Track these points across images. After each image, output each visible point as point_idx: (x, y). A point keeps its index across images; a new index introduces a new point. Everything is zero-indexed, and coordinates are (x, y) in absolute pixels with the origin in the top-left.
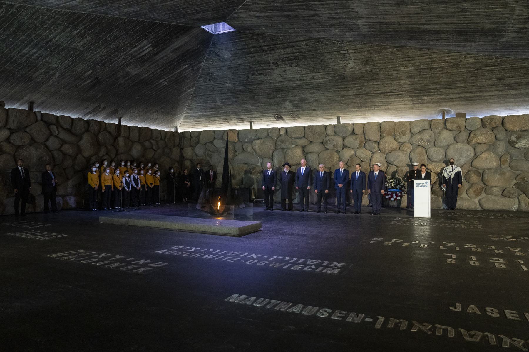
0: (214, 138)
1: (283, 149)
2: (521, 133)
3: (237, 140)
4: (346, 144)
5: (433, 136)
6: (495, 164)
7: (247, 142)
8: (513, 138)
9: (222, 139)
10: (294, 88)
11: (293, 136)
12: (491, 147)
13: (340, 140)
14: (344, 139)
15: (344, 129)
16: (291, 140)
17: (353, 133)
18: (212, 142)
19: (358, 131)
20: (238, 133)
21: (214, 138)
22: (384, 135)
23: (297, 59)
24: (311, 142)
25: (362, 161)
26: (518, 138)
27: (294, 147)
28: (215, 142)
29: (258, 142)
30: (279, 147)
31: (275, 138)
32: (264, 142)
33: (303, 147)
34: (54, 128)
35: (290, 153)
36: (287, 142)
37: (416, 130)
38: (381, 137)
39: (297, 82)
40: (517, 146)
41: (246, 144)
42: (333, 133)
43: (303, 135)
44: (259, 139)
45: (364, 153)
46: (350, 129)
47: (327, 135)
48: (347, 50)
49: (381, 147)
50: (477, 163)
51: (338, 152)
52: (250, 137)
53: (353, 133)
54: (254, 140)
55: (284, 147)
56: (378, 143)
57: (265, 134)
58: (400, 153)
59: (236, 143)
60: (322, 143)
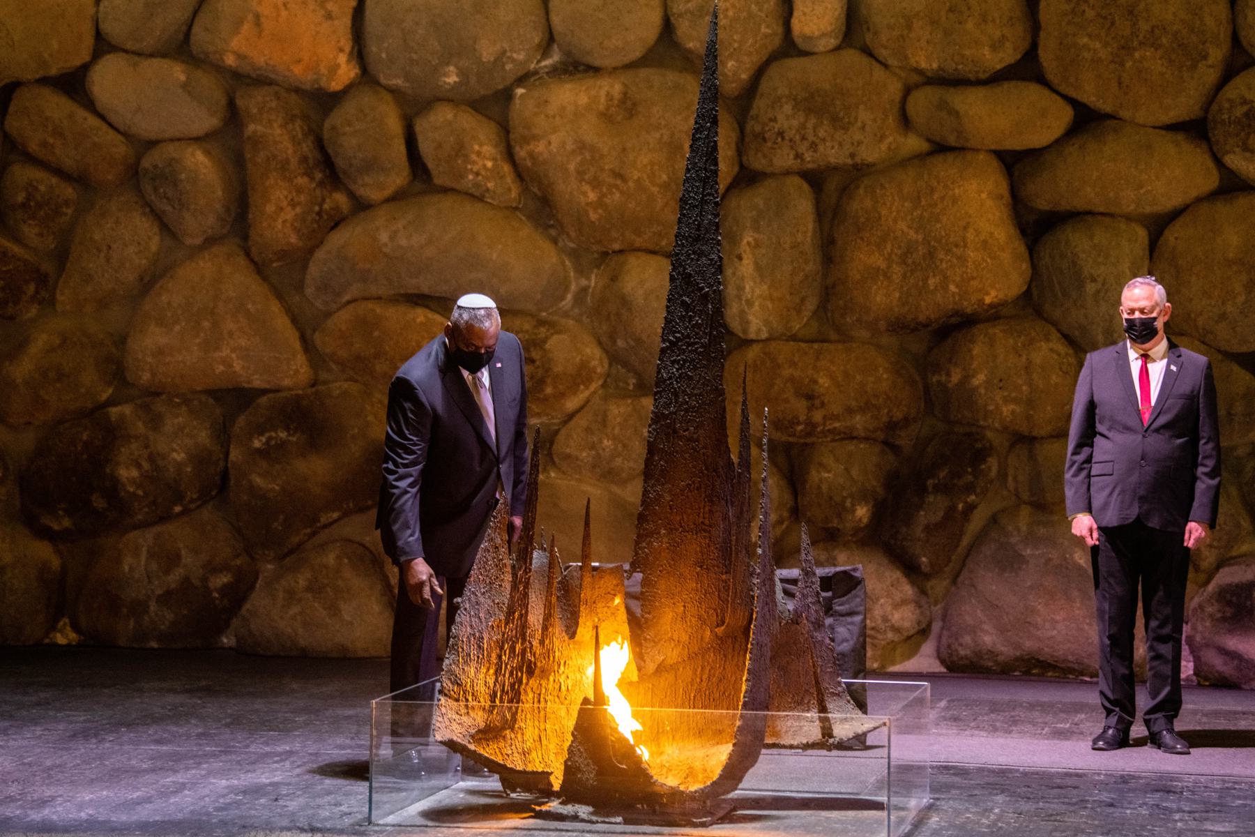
1: (815, 179)
3: (346, 72)
7: (450, 98)
11: (926, 60)
16: (894, 88)
18: (73, 84)
21: (103, 45)
27: (921, 157)
28: (108, 80)
29: (569, 95)
30: (784, 159)
31: (734, 70)
32: (629, 107)
33: (1016, 164)
35: (891, 208)
36: (864, 115)
41: (443, 115)
43: (1008, 56)
44: (577, 67)
52: (487, 52)
54: (521, 80)
55: (833, 153)
59: (324, 101)
60: (1196, 129)
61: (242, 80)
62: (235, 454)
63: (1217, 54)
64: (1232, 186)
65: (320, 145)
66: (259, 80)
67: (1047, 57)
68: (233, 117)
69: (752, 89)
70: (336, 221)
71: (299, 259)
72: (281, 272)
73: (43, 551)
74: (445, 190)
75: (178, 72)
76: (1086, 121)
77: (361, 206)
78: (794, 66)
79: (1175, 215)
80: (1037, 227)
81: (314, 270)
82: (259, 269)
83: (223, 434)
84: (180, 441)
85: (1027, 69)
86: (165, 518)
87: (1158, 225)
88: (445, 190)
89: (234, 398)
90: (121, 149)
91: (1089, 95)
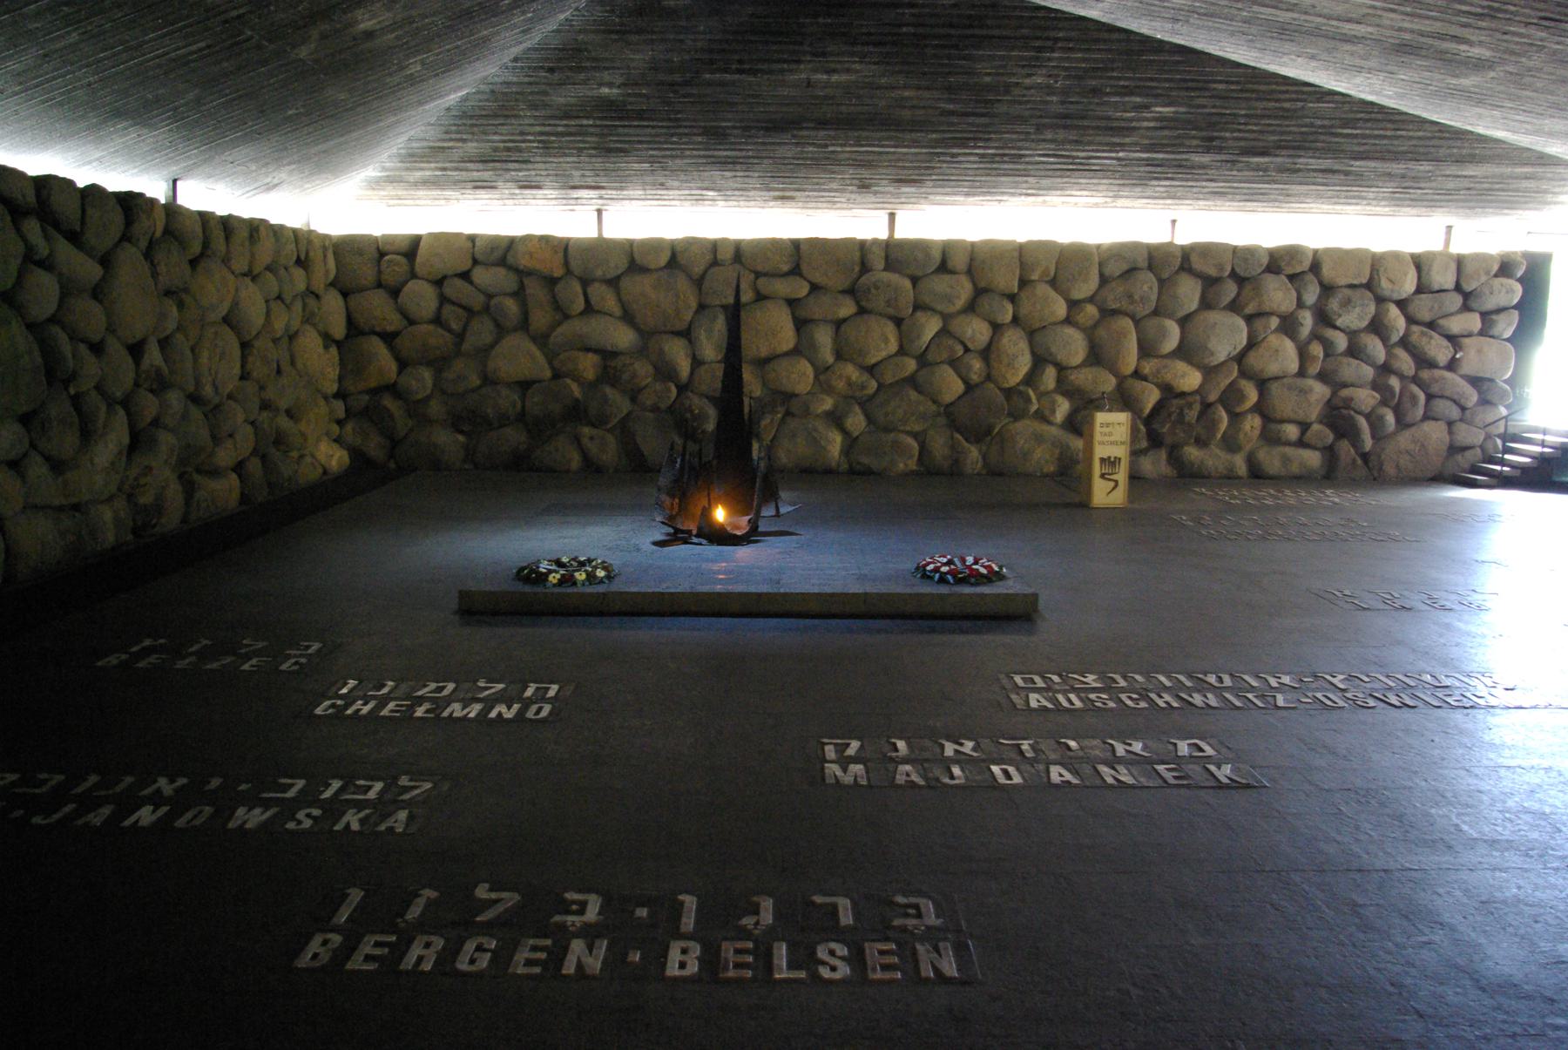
0: (475, 262)
2: (1348, 292)
4: (927, 299)
5: (1156, 290)
6: (1293, 366)
8: (1334, 304)
9: (502, 262)
10: (822, 124)
12: (1288, 326)
13: (907, 284)
14: (915, 280)
15: (920, 256)
17: (944, 267)
19: (959, 262)
20: (564, 248)
22: (1035, 277)
23: (894, 43)
24: (815, 288)
25: (967, 350)
26: (1347, 303)
31: (698, 270)
33: (792, 303)
34: (32, 227)
37: (1114, 269)
38: (1024, 283)
39: (843, 109)
40: (1339, 323)
41: (597, 285)
42: (882, 266)
45: (976, 331)
46: (937, 256)
47: (865, 268)
48: (1056, 40)
49: (1024, 310)
50: (1253, 360)
51: (898, 322)
53: (944, 267)
56: (1012, 298)
57: (664, 259)
58: (1069, 331)
60: (851, 291)
61: (521, 273)
62: (527, 403)
63: (857, 269)
64: (862, 311)
65: (554, 297)
66: (529, 273)
67: (804, 268)
68: (522, 287)
69: (703, 276)
70: (559, 324)
71: (546, 336)
72: (541, 340)
73: (461, 438)
74: (598, 312)
75: (502, 271)
76: (815, 288)
77: (567, 317)
78: (715, 269)
79: (844, 320)
80: (801, 324)
81: (552, 339)
82: (534, 339)
83: (523, 397)
84: (508, 400)
85: (796, 271)
86: (501, 426)
87: (839, 324)
88: (598, 312)
89: (525, 385)
90: (482, 298)
91: (818, 278)
